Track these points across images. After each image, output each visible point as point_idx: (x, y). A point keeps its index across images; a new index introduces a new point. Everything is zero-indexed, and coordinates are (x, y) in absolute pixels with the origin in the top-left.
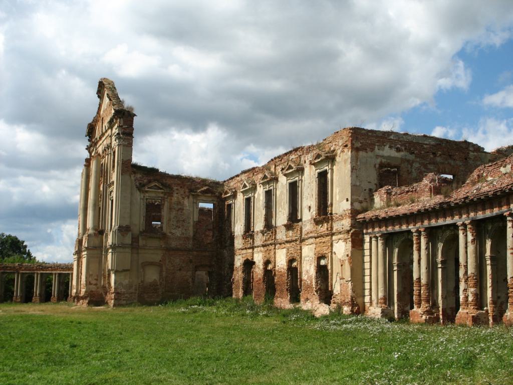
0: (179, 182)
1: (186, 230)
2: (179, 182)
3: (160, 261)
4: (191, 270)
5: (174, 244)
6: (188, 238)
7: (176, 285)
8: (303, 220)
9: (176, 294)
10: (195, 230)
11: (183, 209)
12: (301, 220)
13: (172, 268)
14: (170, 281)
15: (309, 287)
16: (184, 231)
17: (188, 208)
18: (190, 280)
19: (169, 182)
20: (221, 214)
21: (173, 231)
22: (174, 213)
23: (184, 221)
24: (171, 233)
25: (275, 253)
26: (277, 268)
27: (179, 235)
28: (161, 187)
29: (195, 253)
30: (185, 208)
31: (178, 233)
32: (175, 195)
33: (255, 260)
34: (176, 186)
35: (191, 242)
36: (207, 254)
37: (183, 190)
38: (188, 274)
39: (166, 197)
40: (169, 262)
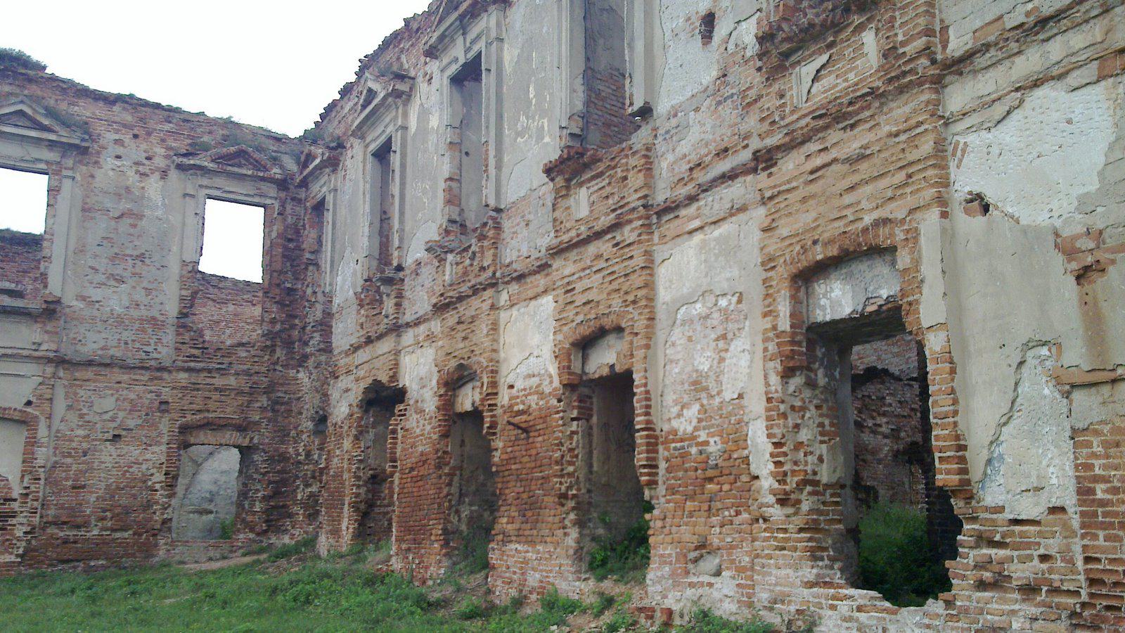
0: (128, 118)
1: (148, 291)
2: (128, 118)
3: (29, 403)
4: (165, 439)
5: (92, 343)
6: (156, 323)
7: (93, 498)
8: (662, 107)
9: (96, 532)
10: (184, 293)
11: (140, 217)
12: (646, 112)
13: (81, 432)
14: (70, 483)
15: (722, 477)
16: (140, 296)
17: (159, 213)
18: (159, 477)
19: (83, 110)
20: (291, 245)
21: (96, 294)
22: (101, 226)
23: (141, 257)
24: (83, 298)
25: (495, 327)
26: (504, 398)
27: (119, 310)
28: (46, 122)
29: (183, 376)
30: (147, 212)
31: (115, 300)
32: (109, 162)
33: (408, 379)
34: (117, 131)
35: (169, 337)
36: (232, 381)
37: (144, 146)
38: (148, 456)
39: (69, 162)
40: (70, 408)
